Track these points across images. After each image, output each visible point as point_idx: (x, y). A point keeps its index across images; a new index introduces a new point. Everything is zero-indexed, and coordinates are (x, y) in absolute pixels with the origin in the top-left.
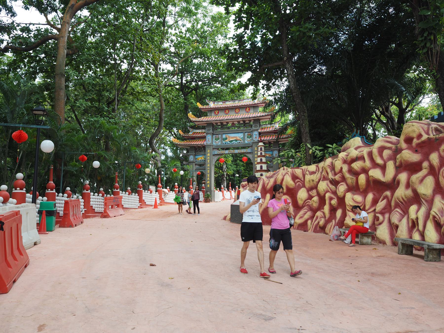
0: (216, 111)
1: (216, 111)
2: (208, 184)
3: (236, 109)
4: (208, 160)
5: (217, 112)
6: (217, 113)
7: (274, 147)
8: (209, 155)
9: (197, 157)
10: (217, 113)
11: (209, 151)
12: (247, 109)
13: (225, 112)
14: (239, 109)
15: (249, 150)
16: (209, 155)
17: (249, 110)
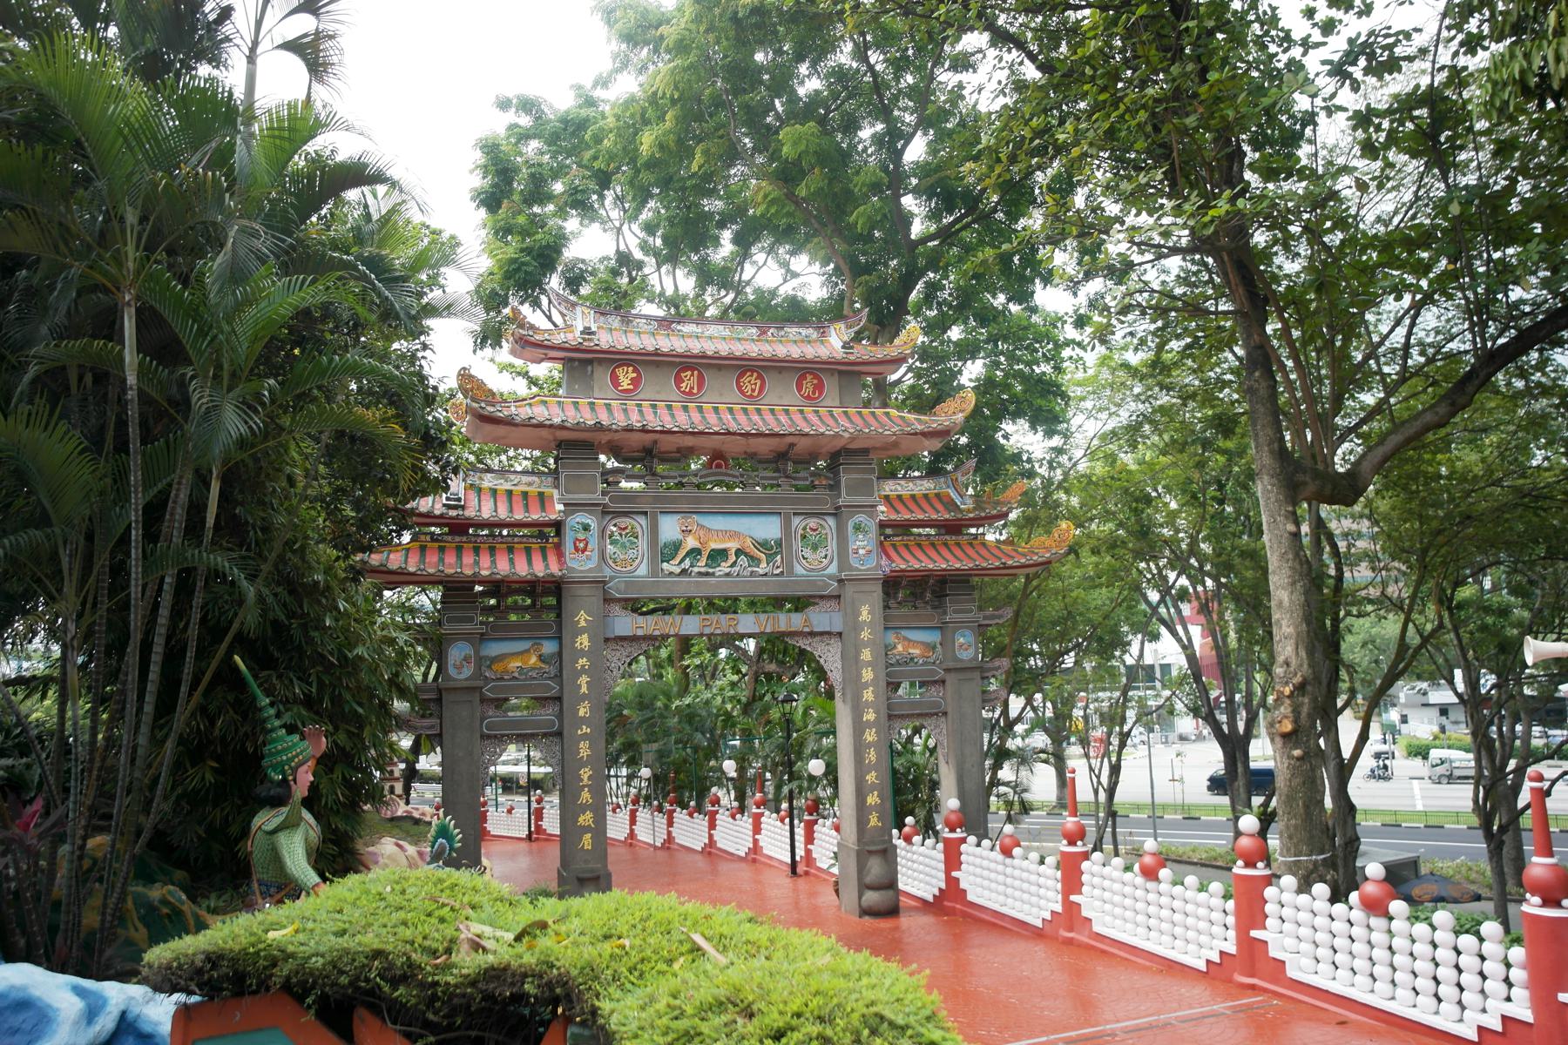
0: (620, 372)
1: (620, 372)
2: (587, 829)
3: (741, 375)
4: (579, 674)
5: (626, 377)
6: (625, 383)
7: (955, 612)
8: (584, 641)
9: (494, 649)
10: (625, 383)
11: (583, 618)
12: (808, 387)
13: (679, 381)
14: (760, 377)
15: (820, 618)
16: (584, 641)
17: (819, 387)
